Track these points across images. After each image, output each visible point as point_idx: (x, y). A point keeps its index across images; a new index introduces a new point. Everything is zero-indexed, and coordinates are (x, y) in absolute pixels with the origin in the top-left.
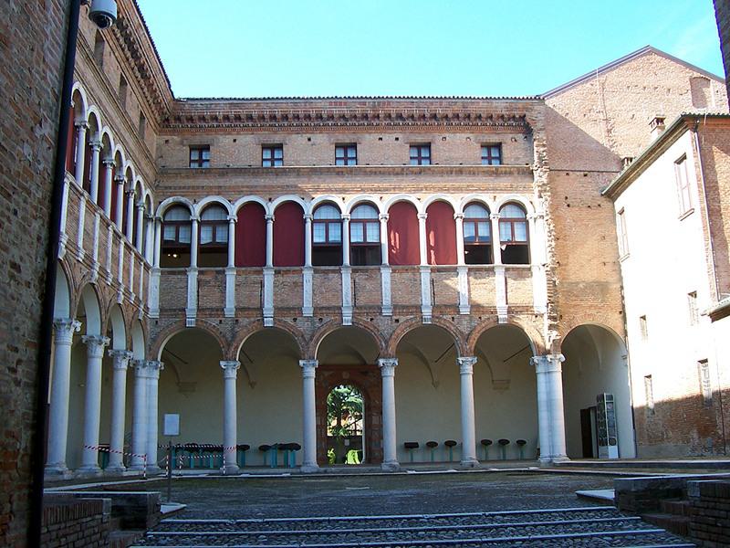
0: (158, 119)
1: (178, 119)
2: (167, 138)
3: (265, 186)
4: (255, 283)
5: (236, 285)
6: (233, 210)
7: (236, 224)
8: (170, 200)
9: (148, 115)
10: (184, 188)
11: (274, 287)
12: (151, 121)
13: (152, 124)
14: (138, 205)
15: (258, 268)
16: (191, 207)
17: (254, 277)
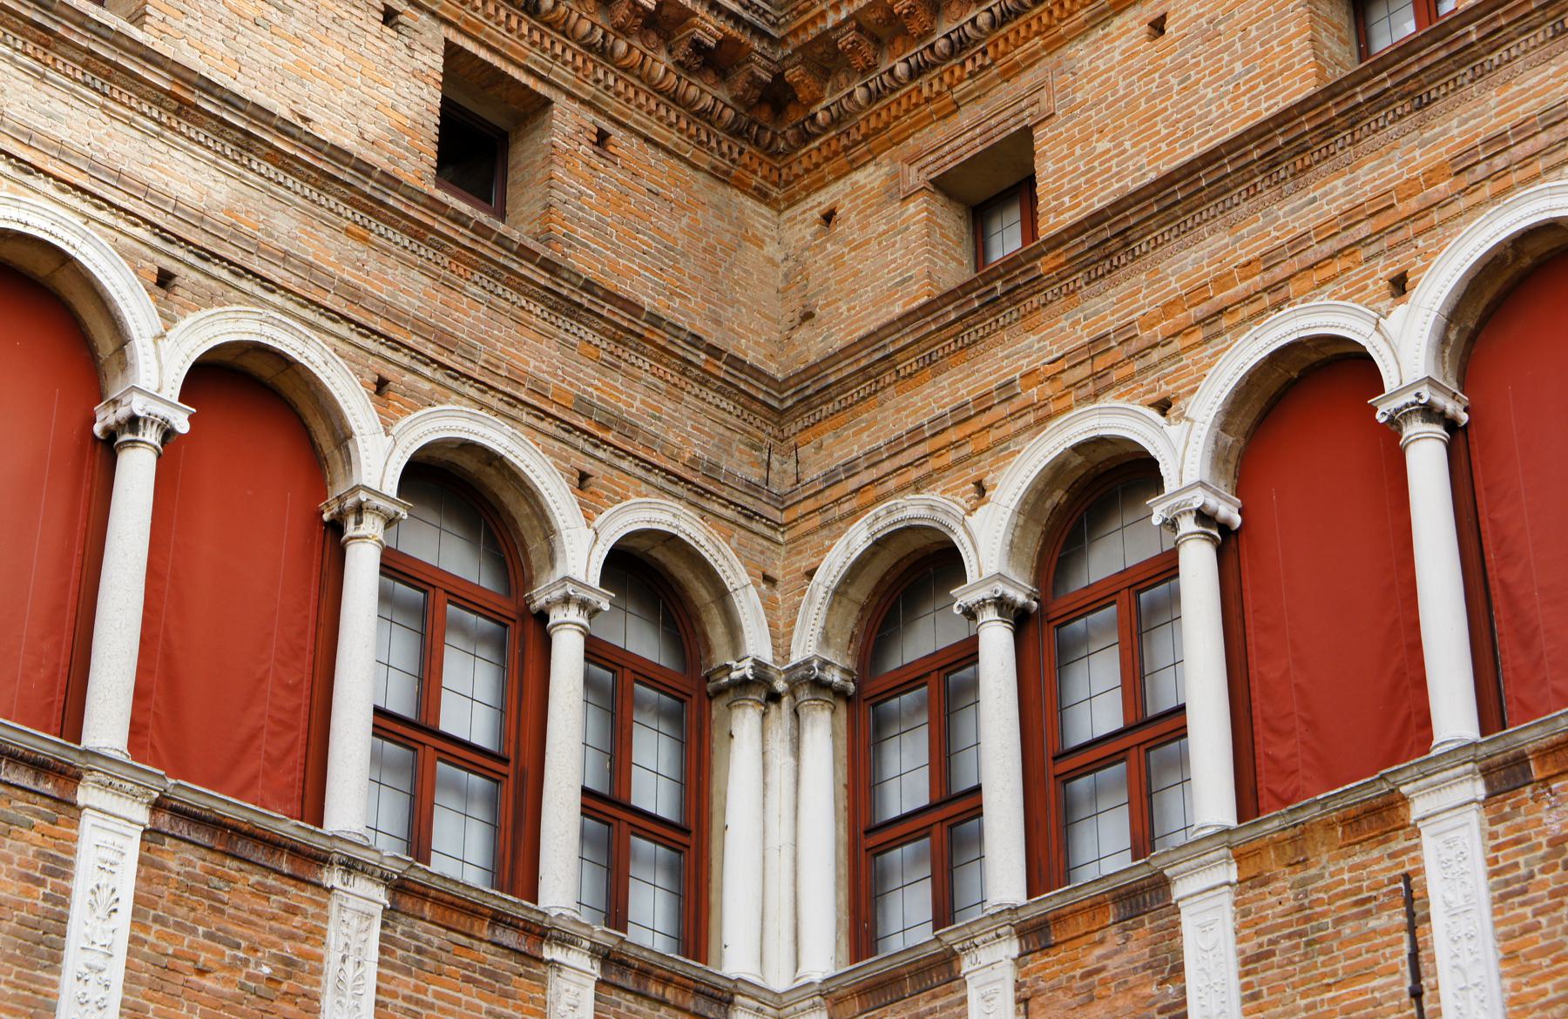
0: (704, 92)
1: (827, 59)
2: (823, 199)
3: (1350, 217)
4: (1365, 906)
5: (1250, 963)
6: (1186, 452)
7: (1227, 542)
8: (857, 538)
9: (563, 74)
10: (915, 436)
11: (1500, 900)
12: (635, 117)
13: (658, 131)
14: (539, 603)
15: (1358, 791)
16: (960, 539)
17: (1340, 869)
